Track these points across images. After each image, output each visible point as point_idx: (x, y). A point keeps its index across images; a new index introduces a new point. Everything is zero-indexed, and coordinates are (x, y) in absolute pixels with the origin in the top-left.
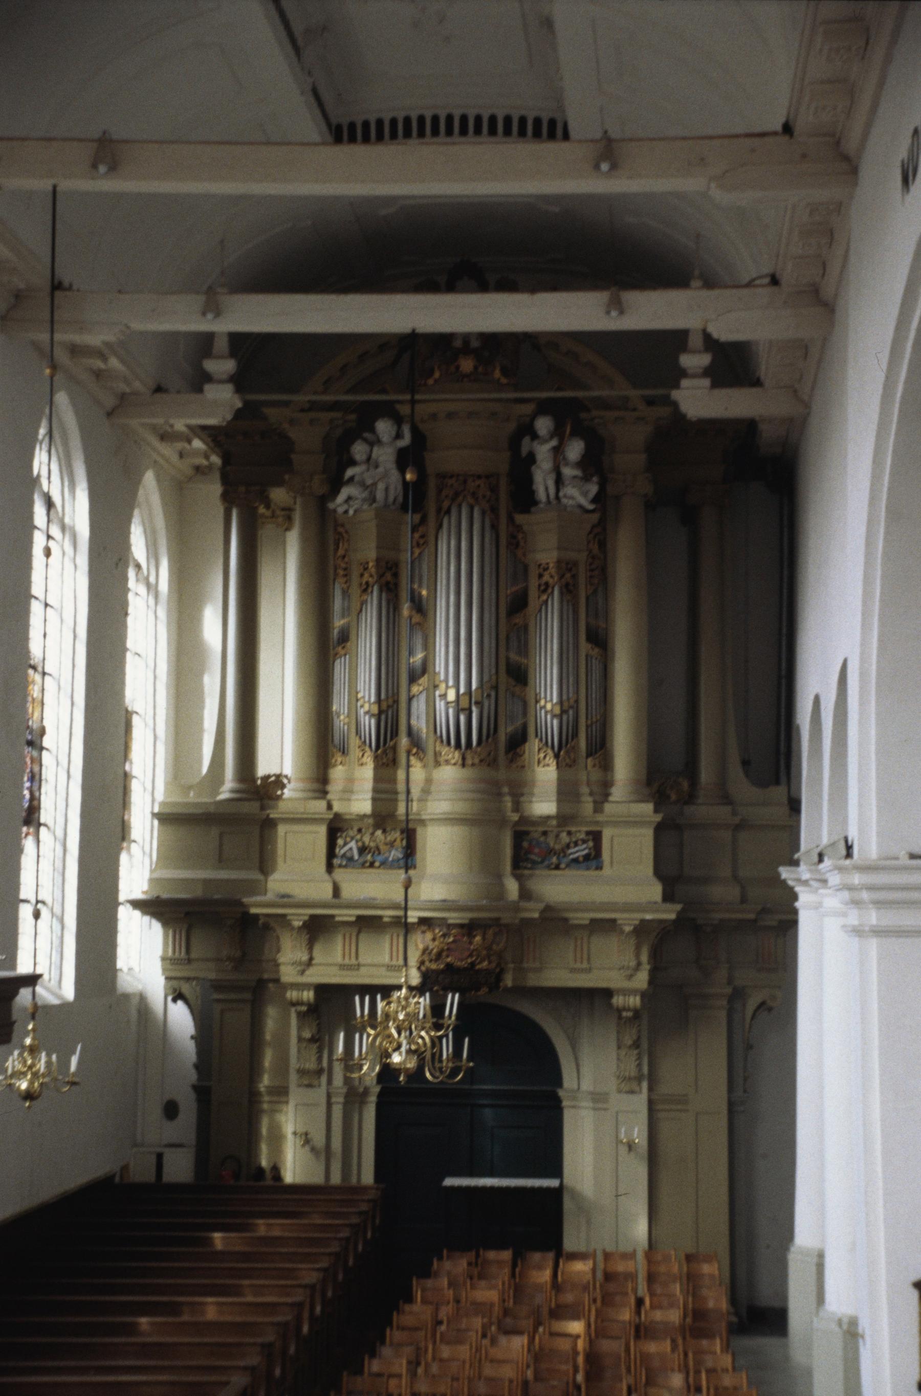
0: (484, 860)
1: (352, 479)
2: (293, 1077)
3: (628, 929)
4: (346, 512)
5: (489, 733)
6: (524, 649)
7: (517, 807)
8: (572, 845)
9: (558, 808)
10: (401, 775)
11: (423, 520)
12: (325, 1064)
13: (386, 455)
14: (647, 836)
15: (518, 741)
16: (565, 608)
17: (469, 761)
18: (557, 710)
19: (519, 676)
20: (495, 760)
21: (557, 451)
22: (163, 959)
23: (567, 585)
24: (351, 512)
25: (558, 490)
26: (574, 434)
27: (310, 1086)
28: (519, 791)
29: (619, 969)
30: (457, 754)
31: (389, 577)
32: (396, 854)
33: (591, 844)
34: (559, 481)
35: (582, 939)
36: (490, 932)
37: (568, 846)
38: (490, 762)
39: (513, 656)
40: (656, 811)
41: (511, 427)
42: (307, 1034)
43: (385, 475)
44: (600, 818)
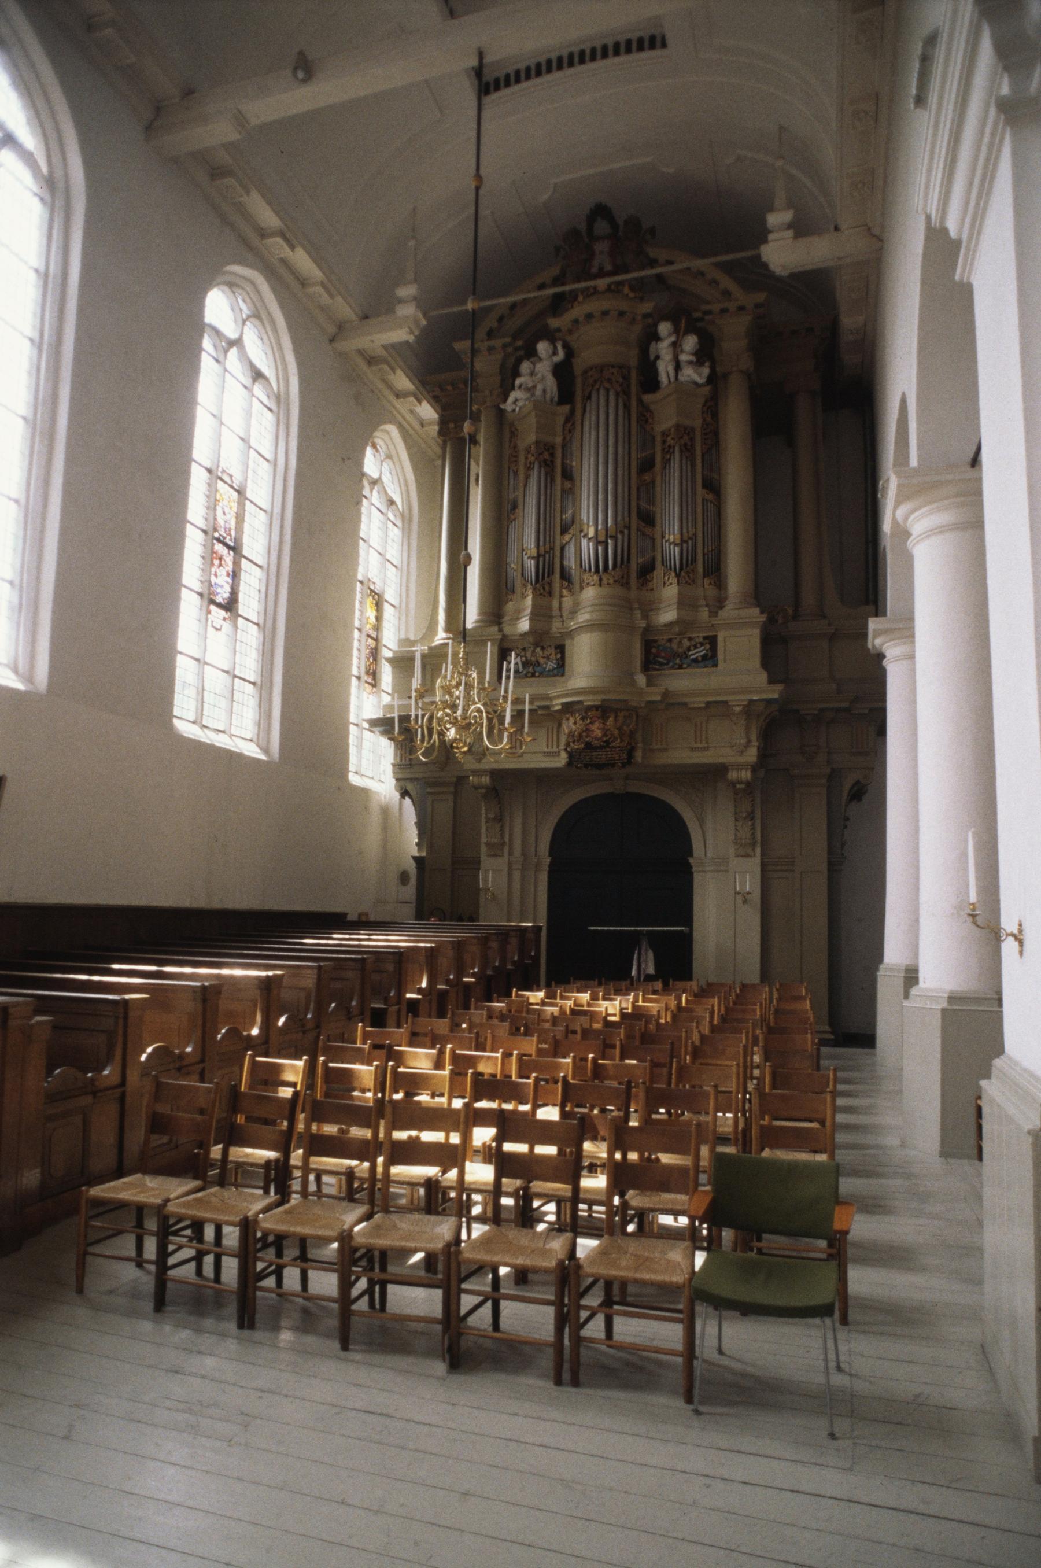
0: (615, 659)
1: (520, 387)
2: (484, 849)
3: (738, 709)
4: (514, 410)
5: (622, 561)
6: (651, 501)
7: (645, 617)
9: (678, 614)
10: (555, 603)
11: (572, 412)
12: (507, 840)
13: (544, 368)
14: (756, 633)
15: (646, 571)
16: (684, 462)
17: (605, 581)
18: (678, 541)
19: (648, 519)
20: (628, 583)
21: (674, 345)
22: (394, 765)
23: (685, 445)
24: (517, 409)
26: (692, 328)
27: (495, 855)
28: (648, 609)
29: (734, 748)
30: (596, 577)
31: (546, 455)
32: (551, 665)
33: (708, 646)
34: (678, 367)
35: (701, 723)
36: (621, 715)
37: (689, 649)
38: (623, 582)
39: (643, 504)
40: (762, 613)
41: (637, 329)
42: (492, 816)
43: (543, 378)
44: (715, 621)
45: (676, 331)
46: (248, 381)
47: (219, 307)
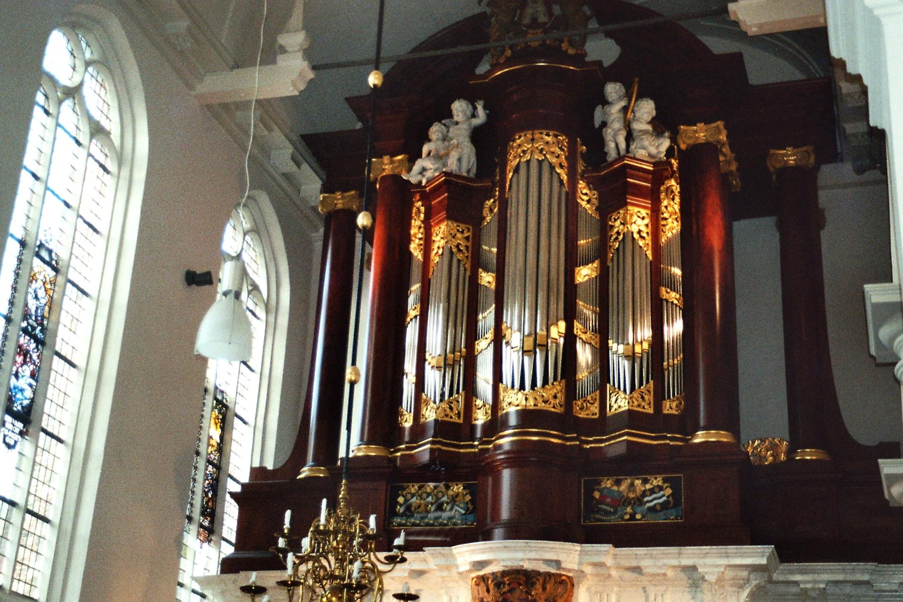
3: (712, 578)
8: (648, 493)
13: (460, 134)
25: (628, 146)
45: (628, 95)
46: (84, 138)
47: (59, 55)
